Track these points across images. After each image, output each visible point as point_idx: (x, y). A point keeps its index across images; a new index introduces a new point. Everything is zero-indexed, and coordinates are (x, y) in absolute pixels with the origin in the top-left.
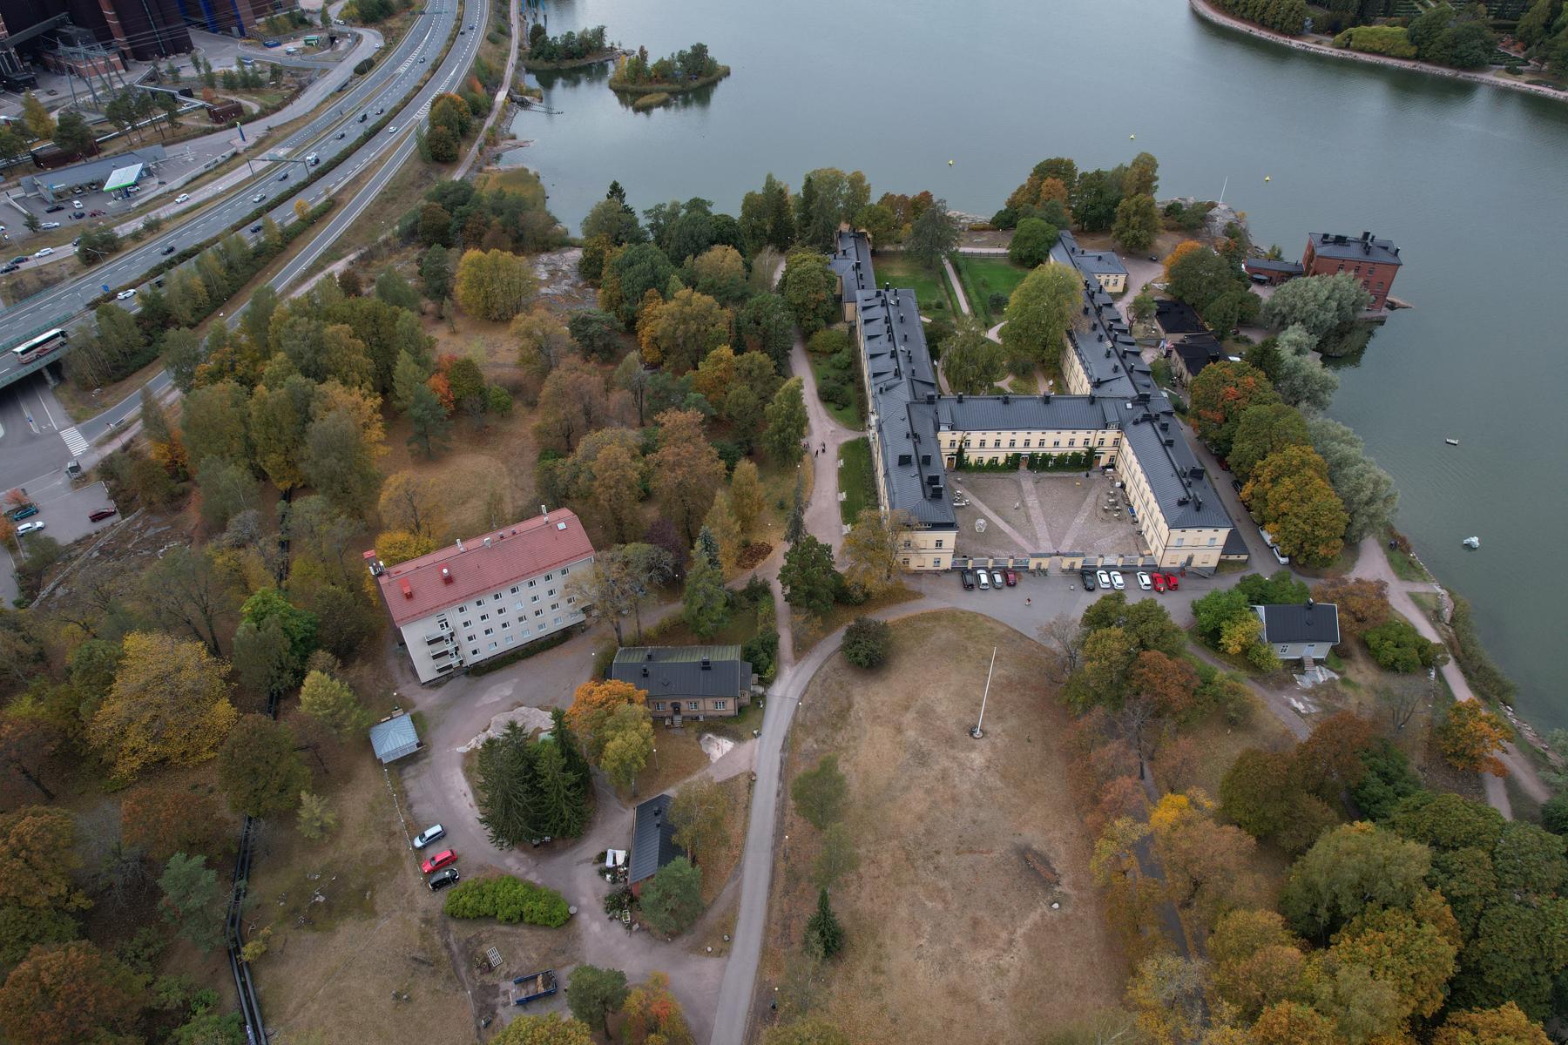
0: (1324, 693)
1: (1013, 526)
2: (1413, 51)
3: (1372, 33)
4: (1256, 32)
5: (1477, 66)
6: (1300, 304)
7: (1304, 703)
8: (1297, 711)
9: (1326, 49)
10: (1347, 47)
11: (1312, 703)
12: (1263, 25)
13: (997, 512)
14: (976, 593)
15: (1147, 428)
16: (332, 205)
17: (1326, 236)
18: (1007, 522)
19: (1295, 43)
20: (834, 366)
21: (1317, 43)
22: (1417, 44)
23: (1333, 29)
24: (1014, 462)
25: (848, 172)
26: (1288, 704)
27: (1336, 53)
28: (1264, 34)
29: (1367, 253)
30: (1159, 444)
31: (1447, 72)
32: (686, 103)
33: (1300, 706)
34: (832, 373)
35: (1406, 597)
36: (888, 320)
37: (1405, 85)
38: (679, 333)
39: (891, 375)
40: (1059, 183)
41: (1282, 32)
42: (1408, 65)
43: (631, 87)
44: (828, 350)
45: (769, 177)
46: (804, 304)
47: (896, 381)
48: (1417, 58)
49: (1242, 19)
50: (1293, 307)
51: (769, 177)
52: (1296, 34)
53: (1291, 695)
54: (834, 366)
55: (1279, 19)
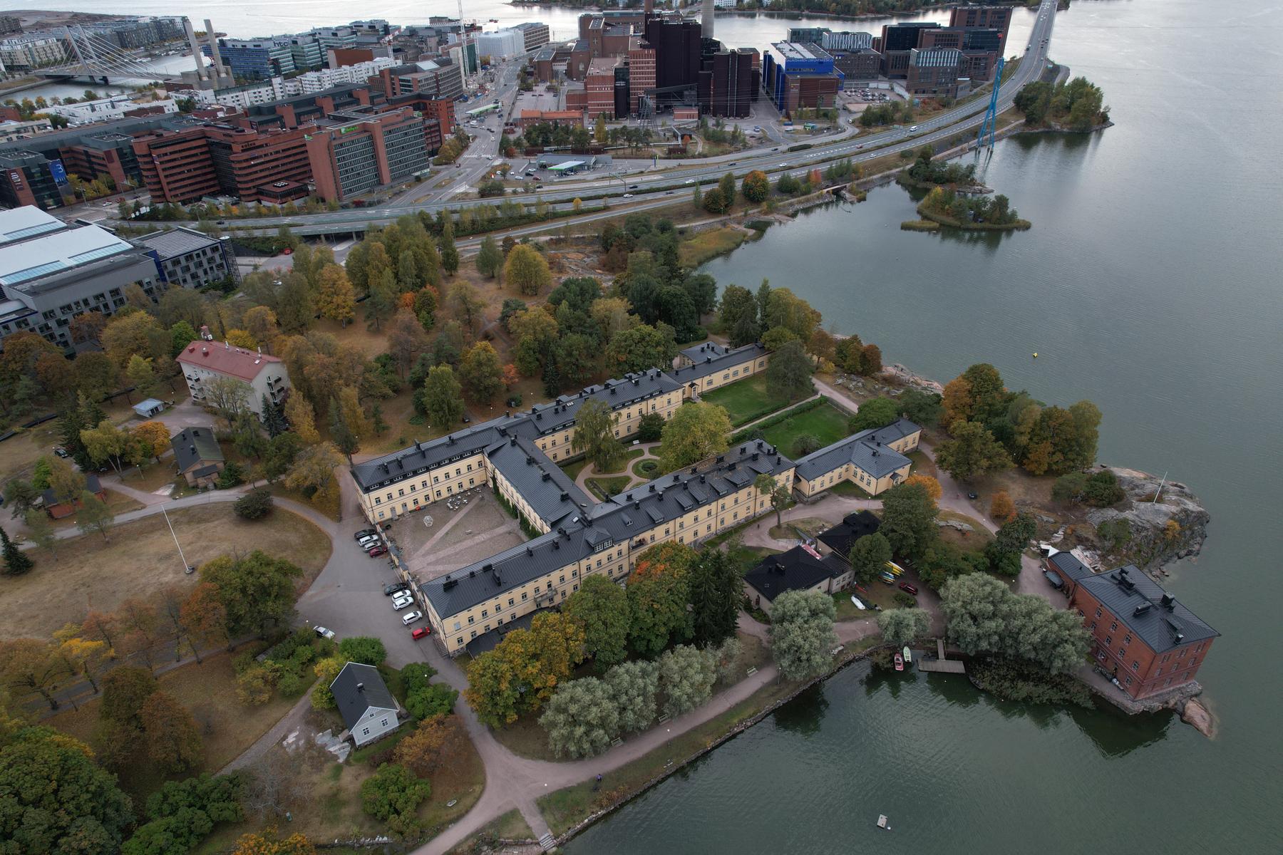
0: (315, 753)
1: (443, 538)
7: (296, 742)
8: (285, 738)
11: (298, 748)
13: (457, 525)
14: (355, 543)
16: (606, 208)
18: (447, 534)
26: (290, 731)
32: (973, 241)
33: (291, 739)
35: (509, 808)
43: (926, 212)
45: (766, 282)
51: (766, 282)
53: (301, 731)
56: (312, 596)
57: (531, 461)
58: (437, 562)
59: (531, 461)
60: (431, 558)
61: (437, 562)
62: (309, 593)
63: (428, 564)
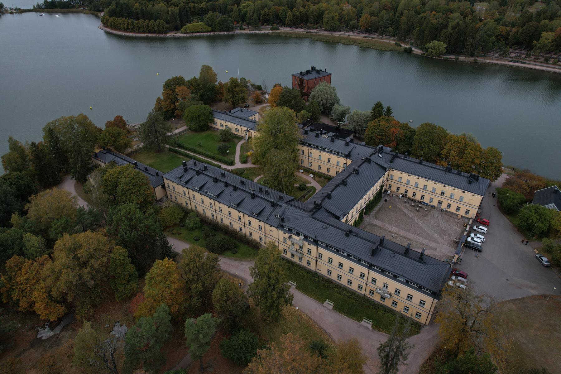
2: (210, 29)
3: (194, 26)
4: (150, 35)
5: (233, 29)
6: (329, 97)
9: (179, 34)
10: (187, 33)
12: (150, 32)
15: (397, 161)
17: (301, 73)
19: (168, 35)
20: (192, 229)
21: (175, 33)
22: (210, 26)
23: (177, 29)
24: (361, 216)
25: (76, 114)
27: (185, 35)
28: (154, 35)
29: (320, 74)
30: (417, 165)
31: (226, 33)
34: (196, 233)
36: (216, 180)
37: (212, 40)
38: (87, 277)
39: (269, 209)
40: (182, 87)
41: (160, 33)
42: (212, 34)
44: (177, 221)
45: (11, 140)
46: (144, 200)
47: (279, 211)
48: (212, 31)
49: (139, 32)
50: (327, 99)
52: (165, 33)
54: (192, 229)
55: (156, 28)
56: (534, 288)
57: (357, 172)
58: (434, 240)
59: (357, 172)
60: (433, 244)
61: (434, 240)
62: (534, 292)
63: (439, 243)
